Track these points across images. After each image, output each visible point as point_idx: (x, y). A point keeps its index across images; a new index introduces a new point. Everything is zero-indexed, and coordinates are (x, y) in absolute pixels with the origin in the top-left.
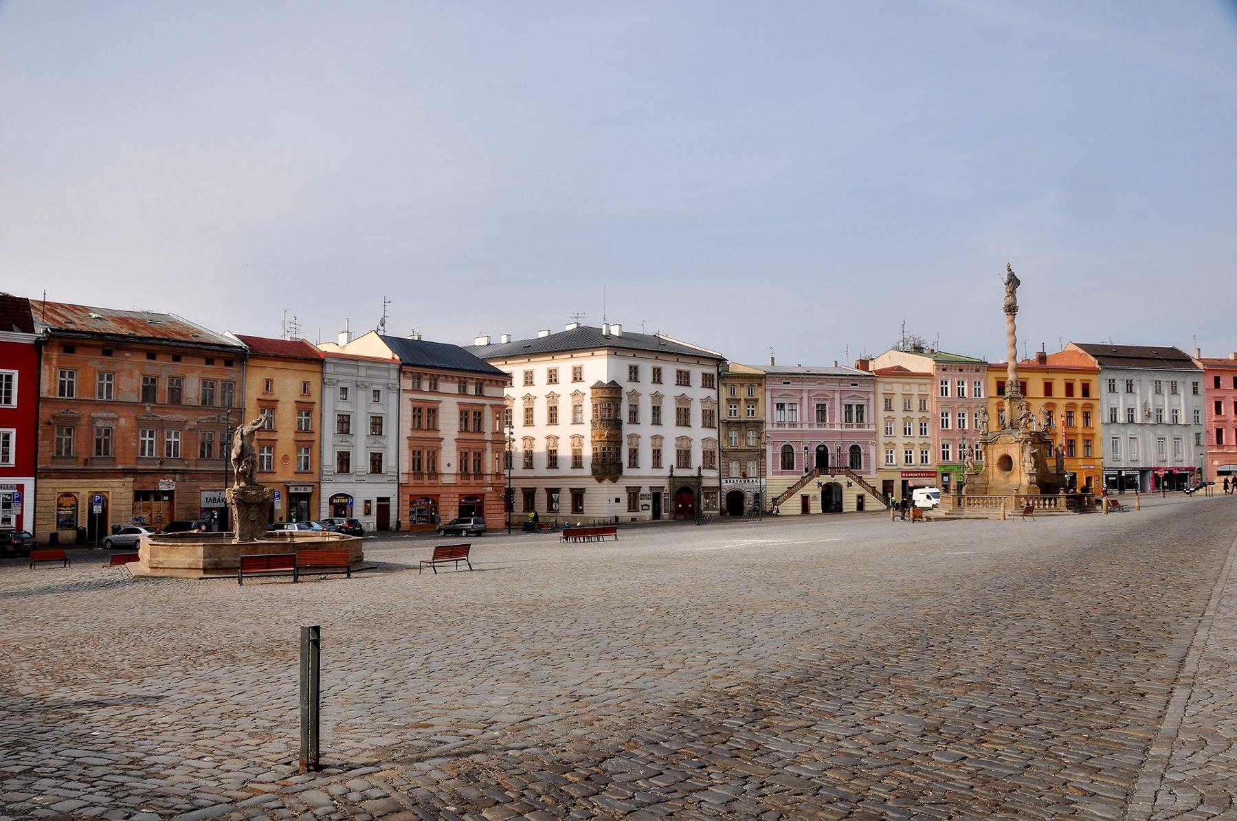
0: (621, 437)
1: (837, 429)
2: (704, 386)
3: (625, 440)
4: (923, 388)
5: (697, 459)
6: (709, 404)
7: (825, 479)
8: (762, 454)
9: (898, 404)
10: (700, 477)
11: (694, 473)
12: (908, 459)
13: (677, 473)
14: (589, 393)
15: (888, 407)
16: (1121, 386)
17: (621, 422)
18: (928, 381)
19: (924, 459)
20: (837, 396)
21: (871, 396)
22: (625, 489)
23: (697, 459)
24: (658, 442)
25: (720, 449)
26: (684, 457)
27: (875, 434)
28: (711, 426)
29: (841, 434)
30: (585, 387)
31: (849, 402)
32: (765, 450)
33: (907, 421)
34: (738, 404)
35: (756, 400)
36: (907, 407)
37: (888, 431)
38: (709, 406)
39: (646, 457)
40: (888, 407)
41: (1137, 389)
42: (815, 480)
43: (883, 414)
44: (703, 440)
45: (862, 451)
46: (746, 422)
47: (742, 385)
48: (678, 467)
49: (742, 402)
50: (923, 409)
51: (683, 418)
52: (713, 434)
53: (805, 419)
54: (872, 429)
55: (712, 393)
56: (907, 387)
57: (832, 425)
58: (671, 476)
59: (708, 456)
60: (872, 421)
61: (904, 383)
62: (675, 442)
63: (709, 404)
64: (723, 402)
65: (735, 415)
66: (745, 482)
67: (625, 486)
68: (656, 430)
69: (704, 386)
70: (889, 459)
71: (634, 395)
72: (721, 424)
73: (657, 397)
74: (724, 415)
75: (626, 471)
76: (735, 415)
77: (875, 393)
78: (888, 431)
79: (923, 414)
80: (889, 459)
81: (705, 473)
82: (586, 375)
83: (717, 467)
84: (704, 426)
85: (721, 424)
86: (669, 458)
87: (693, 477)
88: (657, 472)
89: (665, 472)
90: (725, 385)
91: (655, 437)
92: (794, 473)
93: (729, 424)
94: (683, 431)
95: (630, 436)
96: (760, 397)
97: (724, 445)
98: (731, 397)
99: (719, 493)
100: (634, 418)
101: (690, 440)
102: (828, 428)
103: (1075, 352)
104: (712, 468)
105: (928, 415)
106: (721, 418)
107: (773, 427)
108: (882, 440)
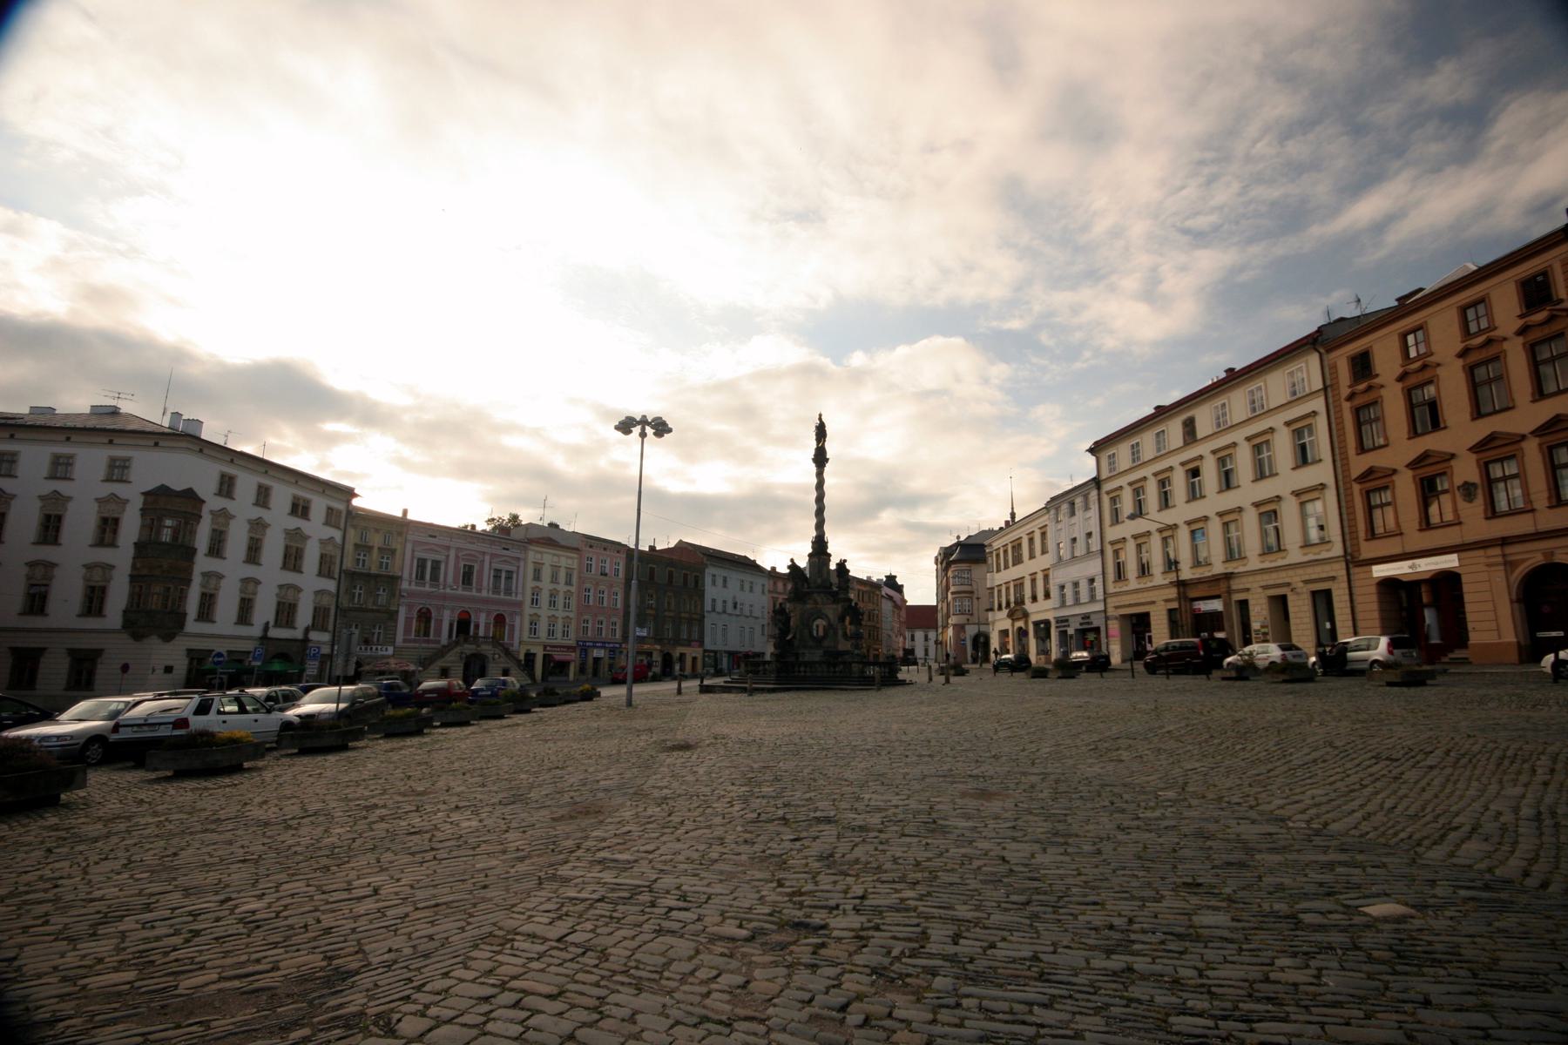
0: (191, 574)
1: (484, 594)
2: (327, 523)
3: (197, 579)
4: (570, 561)
5: (304, 617)
6: (330, 548)
7: (469, 648)
8: (393, 616)
9: (546, 573)
10: (306, 640)
11: (298, 634)
12: (551, 633)
13: (275, 633)
14: (137, 503)
15: (537, 577)
16: (720, 581)
17: (194, 551)
18: (575, 556)
19: (565, 634)
20: (487, 558)
21: (522, 564)
22: (185, 653)
23: (304, 617)
24: (251, 587)
25: (337, 607)
26: (286, 612)
27: (520, 604)
28: (329, 576)
29: (486, 601)
30: (132, 493)
31: (499, 566)
32: (397, 612)
33: (553, 594)
34: (369, 552)
35: (393, 552)
36: (554, 579)
37: (535, 602)
38: (330, 549)
39: (226, 607)
40: (537, 577)
41: (729, 584)
42: (458, 649)
43: (530, 584)
44: (317, 593)
45: (507, 620)
46: (377, 576)
47: (377, 531)
48: (277, 624)
49: (375, 551)
50: (569, 583)
51: (292, 559)
52: (331, 585)
53: (450, 580)
54: (519, 598)
55: (337, 535)
56: (555, 559)
57: (479, 590)
58: (264, 638)
59: (320, 615)
60: (520, 590)
61: (554, 555)
62: (277, 591)
63: (330, 548)
64: (349, 548)
65: (363, 565)
66: (366, 649)
67: (185, 648)
68: (250, 571)
69: (327, 523)
70: (533, 631)
71: (223, 516)
72: (343, 575)
73: (258, 526)
74: (349, 564)
75: (192, 625)
76: (363, 565)
77: (525, 560)
78: (535, 602)
79: (569, 588)
80: (533, 631)
81: (314, 636)
82: (135, 474)
83: (331, 627)
84: (320, 574)
85: (343, 575)
86: (264, 610)
87: (296, 640)
88: (243, 631)
89: (256, 631)
90: (355, 527)
91: (246, 581)
92: (428, 642)
93: (352, 576)
94: (290, 577)
95: (207, 575)
96: (399, 547)
97: (345, 603)
98: (359, 543)
99: (329, 663)
100: (216, 550)
101: (299, 590)
102: (474, 593)
103: (686, 548)
104: (324, 629)
105: (573, 589)
106: (344, 567)
107: (410, 584)
108: (528, 610)
